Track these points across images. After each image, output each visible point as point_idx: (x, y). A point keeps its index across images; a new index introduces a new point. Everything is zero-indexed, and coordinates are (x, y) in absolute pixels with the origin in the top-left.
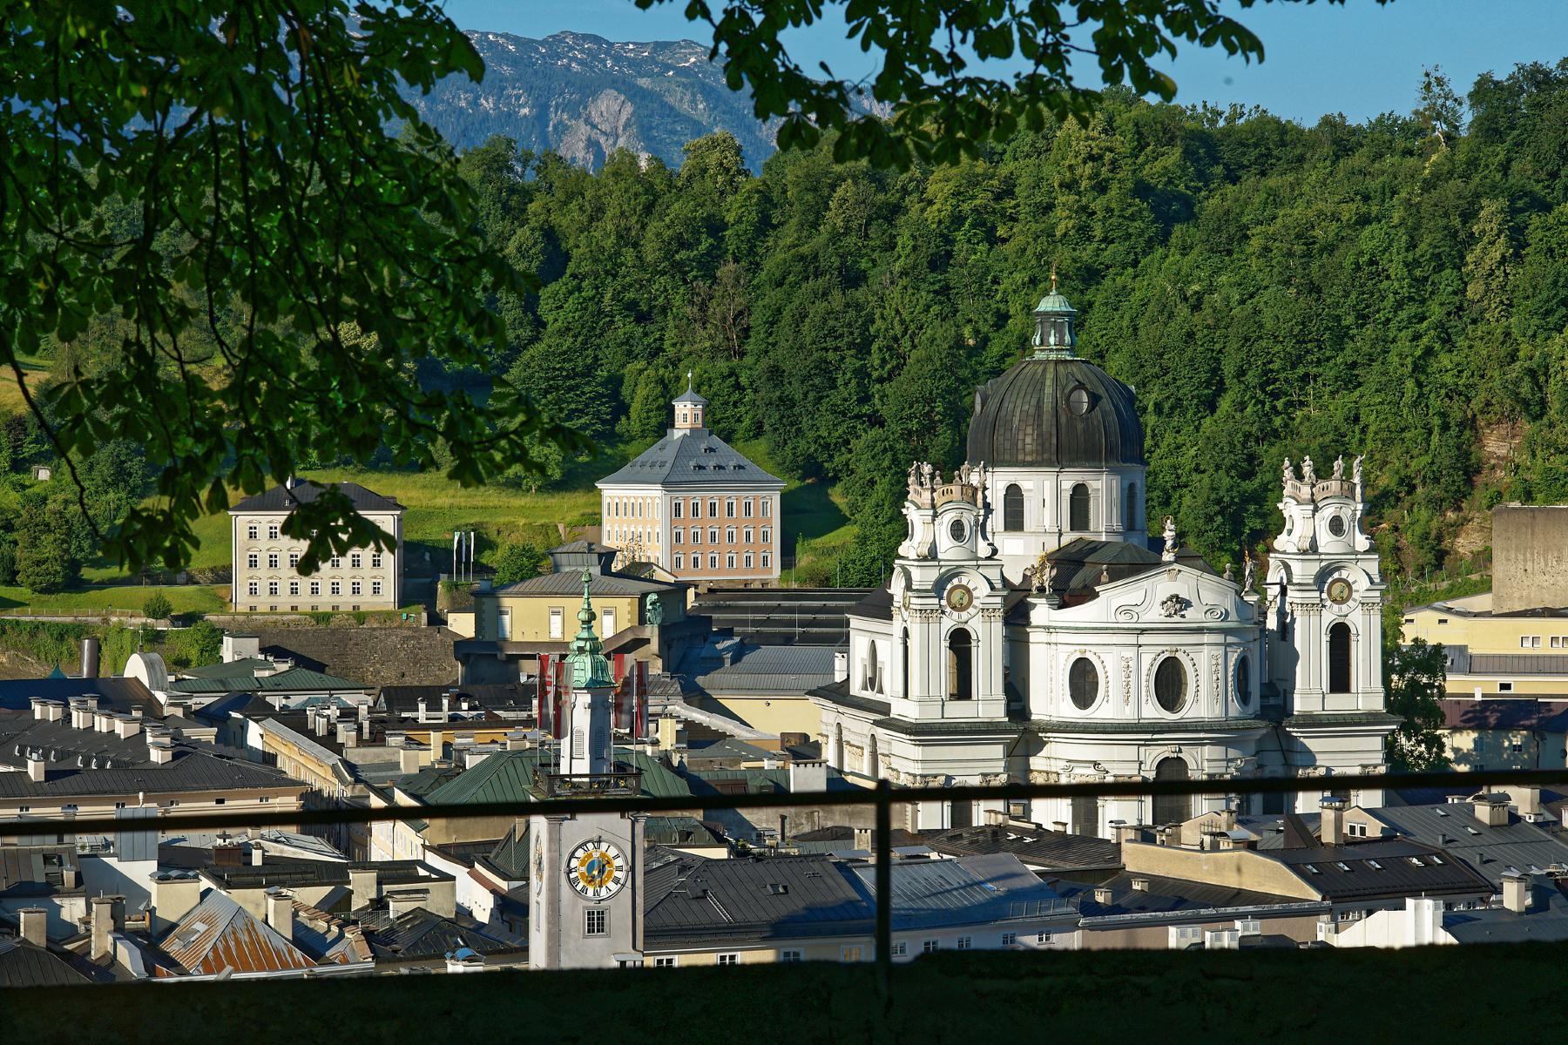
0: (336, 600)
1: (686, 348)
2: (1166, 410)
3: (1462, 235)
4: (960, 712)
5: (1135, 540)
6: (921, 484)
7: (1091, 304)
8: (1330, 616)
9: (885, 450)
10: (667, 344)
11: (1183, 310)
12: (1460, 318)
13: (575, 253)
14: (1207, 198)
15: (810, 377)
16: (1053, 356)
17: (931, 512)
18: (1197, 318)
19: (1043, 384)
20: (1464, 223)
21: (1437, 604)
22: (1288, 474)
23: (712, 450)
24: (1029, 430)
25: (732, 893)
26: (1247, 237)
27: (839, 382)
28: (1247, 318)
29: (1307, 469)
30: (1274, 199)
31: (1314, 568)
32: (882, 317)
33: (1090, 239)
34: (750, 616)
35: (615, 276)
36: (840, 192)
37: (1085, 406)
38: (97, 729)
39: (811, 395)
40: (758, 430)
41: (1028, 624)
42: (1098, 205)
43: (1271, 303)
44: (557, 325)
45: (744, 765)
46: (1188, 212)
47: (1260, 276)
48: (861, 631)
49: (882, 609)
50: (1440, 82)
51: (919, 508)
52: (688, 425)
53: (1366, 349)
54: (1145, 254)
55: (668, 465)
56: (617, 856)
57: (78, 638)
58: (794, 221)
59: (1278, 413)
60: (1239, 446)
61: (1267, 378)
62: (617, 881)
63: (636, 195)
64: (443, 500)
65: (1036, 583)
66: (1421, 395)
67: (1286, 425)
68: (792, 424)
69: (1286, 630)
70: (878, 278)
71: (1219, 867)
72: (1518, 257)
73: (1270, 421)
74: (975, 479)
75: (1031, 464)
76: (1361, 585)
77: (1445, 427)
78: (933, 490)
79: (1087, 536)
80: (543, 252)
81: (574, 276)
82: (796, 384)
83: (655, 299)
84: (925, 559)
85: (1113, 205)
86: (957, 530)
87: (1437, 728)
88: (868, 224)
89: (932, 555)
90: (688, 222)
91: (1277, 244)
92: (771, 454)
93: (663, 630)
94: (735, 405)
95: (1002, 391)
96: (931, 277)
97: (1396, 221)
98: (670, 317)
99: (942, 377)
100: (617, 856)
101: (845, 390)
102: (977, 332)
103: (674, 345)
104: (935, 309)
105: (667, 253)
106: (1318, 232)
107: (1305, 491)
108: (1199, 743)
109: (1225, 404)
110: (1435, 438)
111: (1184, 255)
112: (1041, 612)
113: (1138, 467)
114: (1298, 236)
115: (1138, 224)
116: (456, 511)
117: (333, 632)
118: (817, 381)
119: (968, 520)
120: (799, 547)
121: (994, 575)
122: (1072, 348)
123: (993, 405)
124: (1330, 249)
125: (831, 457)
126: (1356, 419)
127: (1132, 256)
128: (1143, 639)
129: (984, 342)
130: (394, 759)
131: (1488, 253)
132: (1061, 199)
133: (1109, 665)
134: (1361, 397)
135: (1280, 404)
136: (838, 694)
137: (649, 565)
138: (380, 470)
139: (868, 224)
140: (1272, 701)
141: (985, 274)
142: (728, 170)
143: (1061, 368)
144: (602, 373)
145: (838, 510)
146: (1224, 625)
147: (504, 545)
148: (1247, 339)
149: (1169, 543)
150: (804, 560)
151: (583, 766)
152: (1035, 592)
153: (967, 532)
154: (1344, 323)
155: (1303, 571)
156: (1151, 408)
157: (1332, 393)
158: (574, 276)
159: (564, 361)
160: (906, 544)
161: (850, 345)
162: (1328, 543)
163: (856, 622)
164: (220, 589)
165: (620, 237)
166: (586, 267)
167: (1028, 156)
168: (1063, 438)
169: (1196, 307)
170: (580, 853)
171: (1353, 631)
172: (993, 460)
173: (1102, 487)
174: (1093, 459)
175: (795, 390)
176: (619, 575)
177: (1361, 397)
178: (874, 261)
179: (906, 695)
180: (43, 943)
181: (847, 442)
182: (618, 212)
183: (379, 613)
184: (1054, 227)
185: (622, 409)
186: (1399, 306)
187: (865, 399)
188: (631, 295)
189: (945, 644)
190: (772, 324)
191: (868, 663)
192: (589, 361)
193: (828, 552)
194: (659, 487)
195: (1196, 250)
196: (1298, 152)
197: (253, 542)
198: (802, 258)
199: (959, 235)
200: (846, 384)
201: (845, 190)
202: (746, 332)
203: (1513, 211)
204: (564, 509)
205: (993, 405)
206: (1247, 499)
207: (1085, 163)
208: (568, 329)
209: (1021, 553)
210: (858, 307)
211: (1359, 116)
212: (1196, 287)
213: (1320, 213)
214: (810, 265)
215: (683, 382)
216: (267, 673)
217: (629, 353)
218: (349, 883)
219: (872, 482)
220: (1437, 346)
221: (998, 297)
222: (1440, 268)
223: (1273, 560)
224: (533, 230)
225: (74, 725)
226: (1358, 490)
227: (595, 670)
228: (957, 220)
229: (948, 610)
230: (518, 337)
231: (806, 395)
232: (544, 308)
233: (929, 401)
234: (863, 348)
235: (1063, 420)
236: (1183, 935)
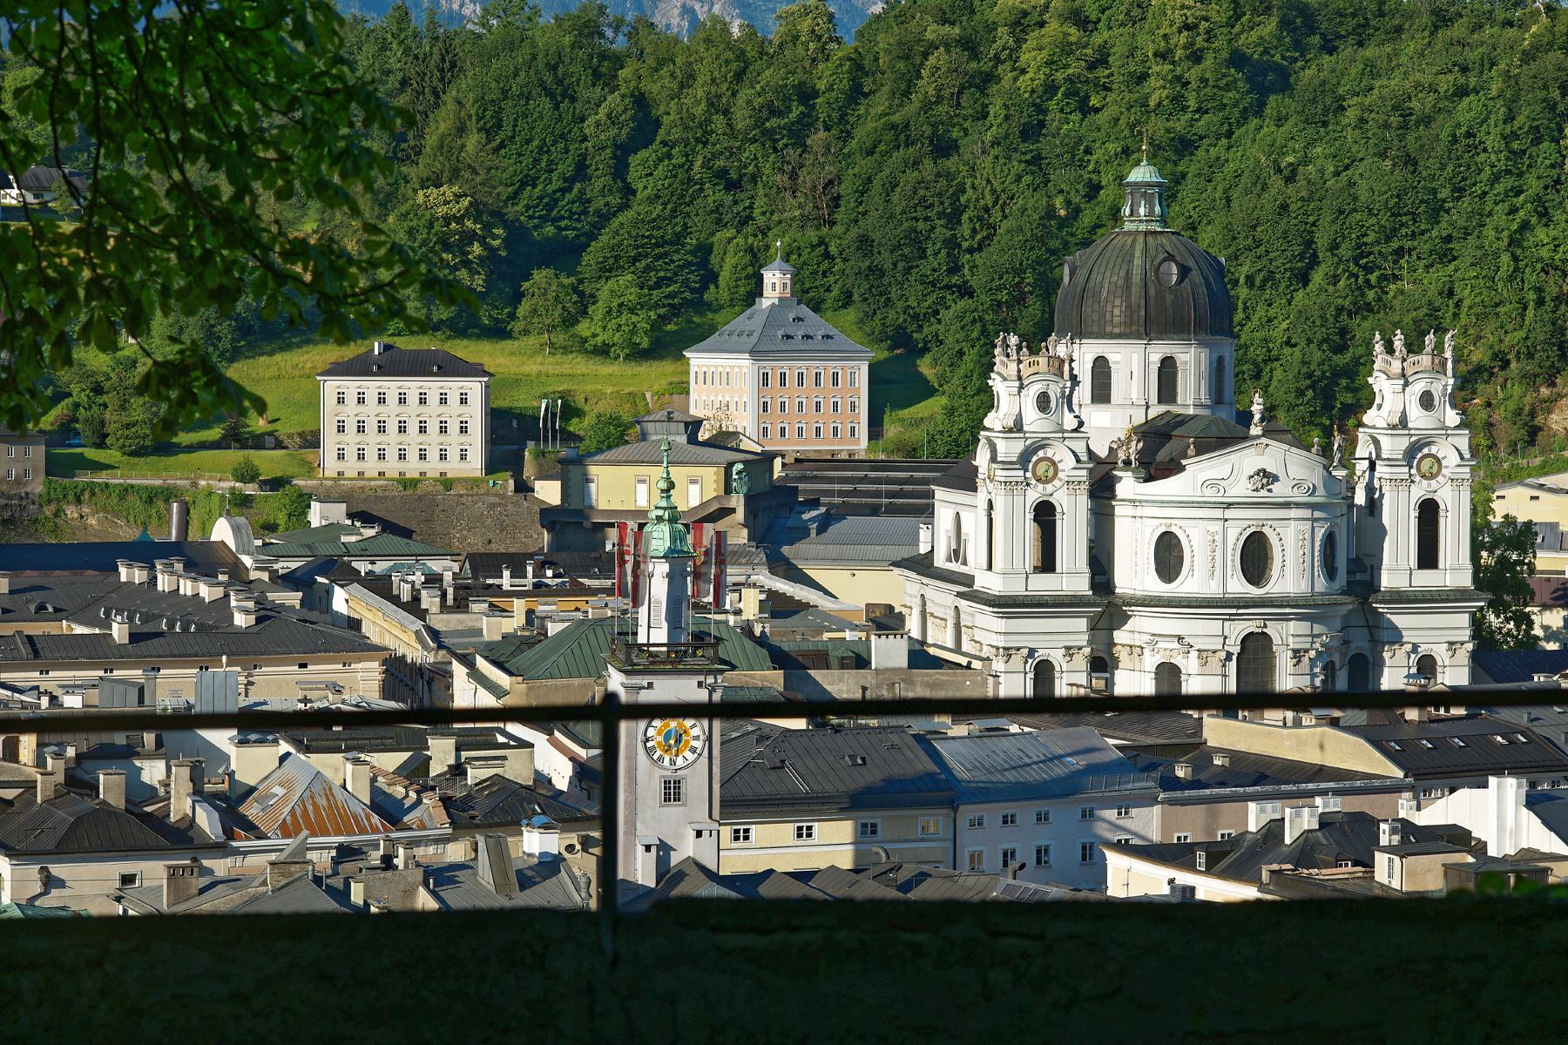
0: (423, 466)
1: (775, 217)
2: (1258, 283)
4: (1043, 584)
5: (1223, 414)
6: (1008, 356)
7: (1184, 175)
8: (1419, 491)
10: (757, 212)
11: (1276, 182)
12: (1558, 191)
13: (666, 120)
14: (1303, 69)
15: (899, 247)
16: (1142, 227)
17: (1017, 384)
18: (1290, 191)
19: (1132, 255)
21: (1528, 481)
22: (1379, 348)
23: (800, 319)
24: (1118, 302)
25: (810, 764)
26: (1343, 108)
27: (929, 252)
28: (1342, 190)
29: (1398, 344)
30: (1371, 69)
31: (1404, 443)
32: (973, 187)
33: (1184, 109)
34: (837, 487)
35: (705, 144)
36: (932, 60)
37: (1175, 278)
38: (182, 592)
39: (901, 265)
40: (847, 300)
41: (1113, 497)
42: (1193, 75)
43: (1366, 175)
45: (826, 636)
46: (1284, 82)
47: (1355, 148)
48: (946, 501)
49: (967, 481)
51: (1005, 379)
52: (777, 294)
53: (1461, 223)
54: (1239, 125)
55: (756, 335)
57: (167, 501)
58: (886, 89)
59: (1371, 287)
60: (1331, 320)
61: (1361, 252)
62: (693, 750)
63: (727, 62)
64: (531, 367)
65: (1122, 455)
66: (1516, 269)
67: (1380, 299)
68: (881, 294)
69: (1373, 506)
70: (970, 147)
71: (1301, 743)
73: (1363, 295)
74: (1062, 351)
75: (1119, 336)
76: (1451, 460)
77: (1540, 302)
78: (1020, 362)
79: (1174, 409)
80: (633, 119)
81: (664, 143)
82: (886, 254)
83: (745, 167)
84: (1010, 431)
85: (1208, 75)
86: (1043, 402)
87: (1526, 605)
88: (960, 93)
89: (1018, 427)
90: (779, 90)
91: (1373, 115)
92: (861, 322)
93: (749, 500)
94: (824, 274)
95: (1091, 263)
96: (1023, 147)
97: (1494, 93)
98: (760, 185)
99: (1033, 248)
101: (936, 260)
102: (1068, 202)
103: (764, 213)
104: (1027, 179)
106: (1414, 104)
107: (1396, 366)
108: (1285, 618)
109: (1318, 277)
110: (1530, 313)
111: (1278, 126)
112: (1127, 485)
113: (1230, 340)
114: (1395, 108)
116: (543, 379)
117: (420, 498)
119: (1054, 391)
120: (886, 419)
121: (1080, 448)
122: (1163, 220)
123: (1081, 277)
124: (1427, 121)
125: (921, 327)
126: (1451, 293)
127: (1226, 127)
128: (1229, 513)
129: (1076, 212)
130: (477, 625)
133: (1196, 538)
134: (1456, 271)
135: (1373, 278)
136: (922, 565)
137: (736, 434)
138: (469, 337)
139: (960, 93)
140: (1359, 577)
142: (820, 37)
143: (1150, 239)
144: (691, 241)
145: (925, 381)
146: (1311, 499)
147: (592, 413)
148: (1341, 212)
149: (1257, 417)
150: (891, 430)
151: (660, 635)
152: (1121, 465)
153: (1053, 404)
154: (1440, 196)
155: (1393, 446)
156: (1242, 280)
157: (1427, 267)
158: (664, 143)
160: (992, 415)
161: (941, 215)
162: (1419, 418)
163: (940, 493)
164: (308, 454)
166: (676, 134)
167: (1122, 25)
168: (1152, 311)
169: (1290, 179)
171: (1442, 507)
172: (1081, 332)
173: (1191, 359)
174: (1182, 332)
175: (885, 259)
176: (706, 444)
177: (1456, 271)
178: (965, 130)
179: (990, 568)
180: (122, 805)
181: (937, 312)
182: (708, 78)
183: (466, 480)
184: (1147, 97)
185: (711, 277)
186: (1496, 178)
187: (955, 269)
188: (720, 163)
189: (1030, 516)
190: (862, 193)
191: (953, 534)
192: (678, 229)
193: (917, 423)
194: (747, 356)
195: (1291, 122)
197: (341, 407)
198: (893, 127)
199: (1052, 105)
201: (938, 58)
202: (836, 200)
204: (651, 377)
205: (1081, 277)
206: (1339, 373)
207: (1180, 32)
208: (658, 197)
209: (1108, 426)
210: (949, 176)
212: (1290, 159)
213: (1418, 85)
214: (900, 134)
215: (772, 251)
216: (353, 539)
217: (719, 221)
218: (428, 749)
219: (961, 353)
220: (1534, 220)
221: (1090, 168)
222: (1537, 141)
223: (1362, 435)
224: (623, 96)
225: (160, 588)
226: (1449, 365)
227: (673, 539)
228: (1051, 88)
229: (1033, 482)
230: (607, 204)
231: (895, 264)
232: (634, 174)
233: (1019, 272)
234: (953, 218)
235: (1152, 292)
236: (1262, 811)
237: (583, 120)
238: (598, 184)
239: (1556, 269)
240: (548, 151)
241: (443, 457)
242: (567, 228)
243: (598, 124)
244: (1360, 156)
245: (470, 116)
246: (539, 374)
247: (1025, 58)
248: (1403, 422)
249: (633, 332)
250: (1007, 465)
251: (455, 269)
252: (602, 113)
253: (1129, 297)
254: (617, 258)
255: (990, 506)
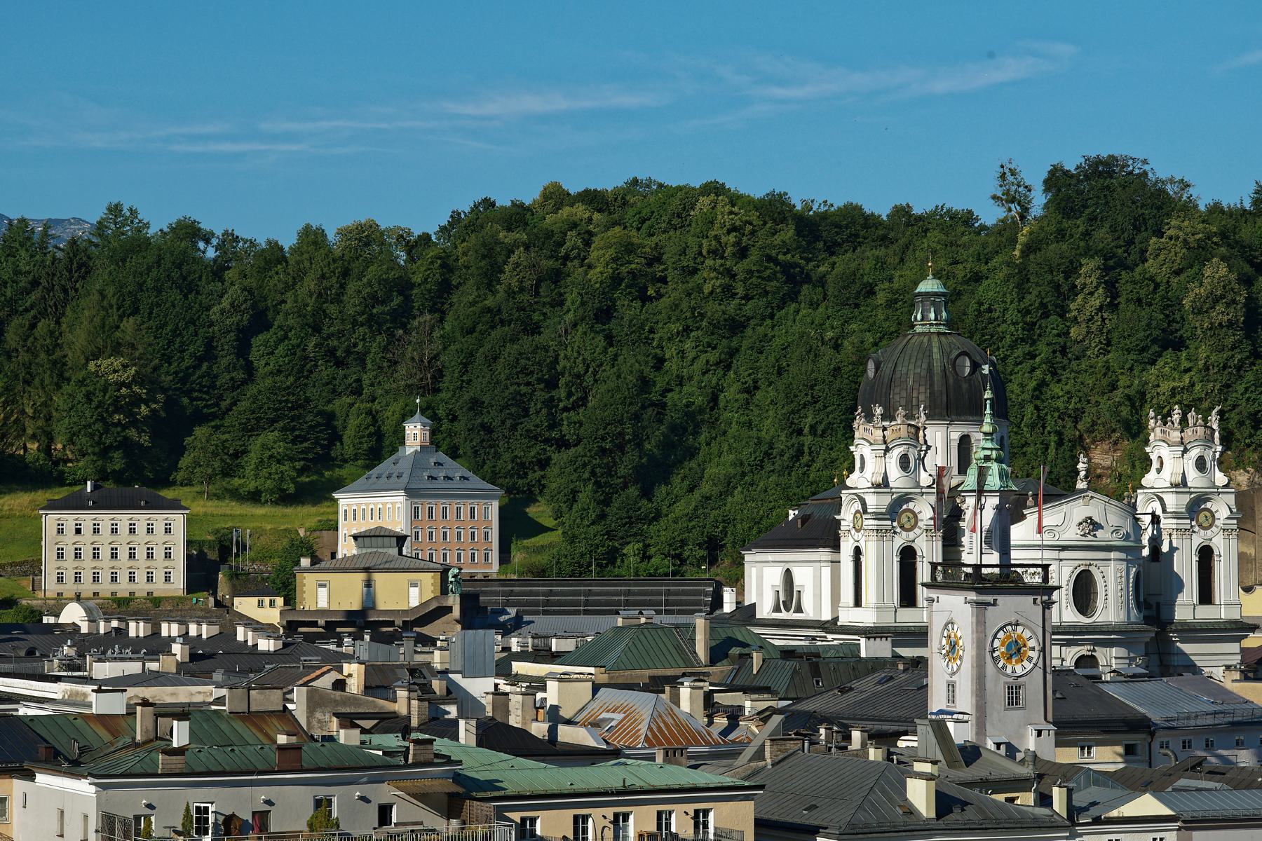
0: (132, 587)
2: (819, 432)
3: (1065, 288)
7: (737, 350)
9: (585, 465)
15: (507, 407)
19: (931, 351)
20: (1066, 278)
23: (440, 464)
24: (922, 389)
27: (532, 411)
36: (514, 258)
37: (967, 370)
39: (508, 423)
42: (740, 268)
44: (268, 368)
49: (829, 537)
50: (1013, 172)
54: (780, 308)
56: (1030, 638)
66: (1039, 416)
72: (1113, 307)
77: (1060, 443)
84: (878, 486)
95: (895, 358)
99: (631, 404)
100: (1030, 638)
101: (537, 419)
105: (367, 306)
107: (1175, 435)
110: (1052, 451)
115: (774, 283)
118: (513, 410)
123: (887, 369)
125: (526, 474)
127: (769, 310)
128: (1064, 555)
131: (1087, 303)
132: (709, 262)
141: (642, 327)
143: (943, 338)
149: (1082, 474)
153: (912, 464)
156: (806, 430)
159: (289, 394)
161: (540, 380)
162: (1195, 479)
165: (320, 295)
169: (837, 347)
170: (1001, 635)
185: (336, 437)
186: (1012, 347)
196: (881, 232)
197: (60, 538)
198: (489, 310)
200: (538, 412)
201: (518, 255)
203: (1106, 269)
204: (301, 519)
207: (729, 232)
211: (920, 208)
214: (494, 317)
219: (574, 492)
221: (655, 344)
222: (1046, 315)
228: (616, 280)
230: (232, 379)
231: (503, 422)
232: (254, 354)
234: (552, 384)
235: (951, 381)
237: (208, 309)
238: (224, 362)
239: (1070, 416)
240: (180, 334)
241: (150, 579)
242: (198, 399)
243: (223, 312)
244: (892, 329)
245: (111, 306)
246: (205, 514)
247: (594, 255)
248: (1184, 482)
249: (282, 479)
250: (878, 516)
251: (125, 427)
252: (225, 303)
253: (931, 386)
254: (258, 419)
255: (858, 551)
